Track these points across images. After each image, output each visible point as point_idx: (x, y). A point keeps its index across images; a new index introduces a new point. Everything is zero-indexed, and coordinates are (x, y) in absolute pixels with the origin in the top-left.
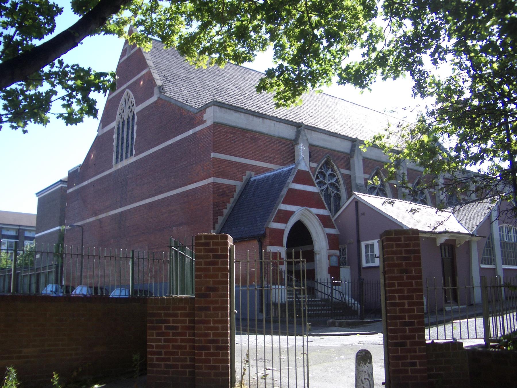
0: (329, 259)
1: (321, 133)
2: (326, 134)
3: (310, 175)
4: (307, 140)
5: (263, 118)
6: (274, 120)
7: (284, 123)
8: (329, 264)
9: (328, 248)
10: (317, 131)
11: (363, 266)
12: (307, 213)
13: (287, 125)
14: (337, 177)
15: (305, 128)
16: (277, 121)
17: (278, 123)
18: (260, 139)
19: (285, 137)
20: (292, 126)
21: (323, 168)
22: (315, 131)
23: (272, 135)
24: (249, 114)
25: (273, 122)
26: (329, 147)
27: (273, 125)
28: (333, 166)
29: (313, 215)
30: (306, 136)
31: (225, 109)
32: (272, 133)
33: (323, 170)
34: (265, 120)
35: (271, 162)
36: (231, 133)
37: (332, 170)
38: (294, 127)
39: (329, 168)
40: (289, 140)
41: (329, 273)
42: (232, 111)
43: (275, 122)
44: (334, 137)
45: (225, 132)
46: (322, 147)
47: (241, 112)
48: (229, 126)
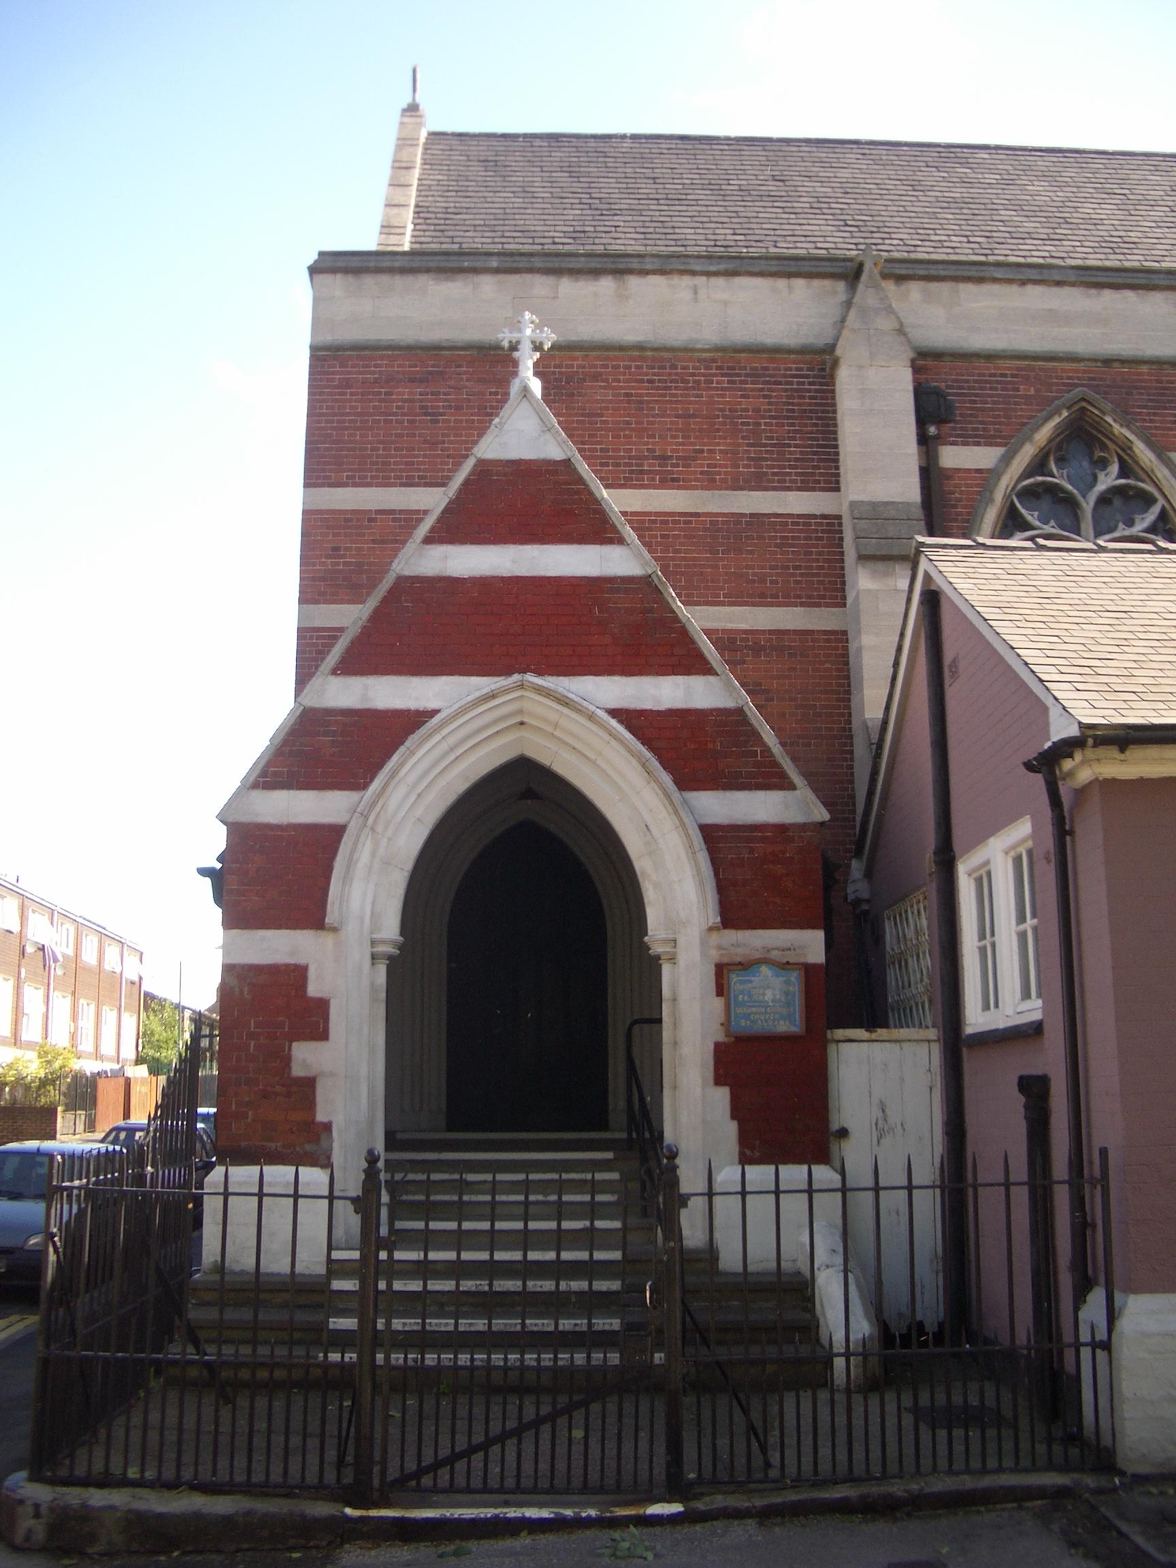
0: (721, 989)
1: (1023, 283)
2: (1059, 284)
3: (581, 480)
4: (901, 331)
5: (620, 272)
6: (693, 273)
7: (761, 274)
8: (726, 1024)
9: (715, 919)
10: (995, 280)
11: (969, 1030)
12: (544, 709)
13: (781, 283)
14: (1161, 502)
15: (885, 276)
16: (708, 274)
17: (720, 282)
18: (596, 377)
19: (769, 340)
20: (816, 283)
21: (1053, 466)
22: (980, 280)
23: (676, 344)
24: (531, 271)
25: (687, 281)
26: (1080, 348)
27: (687, 295)
28: (1127, 447)
29: (591, 717)
30: (890, 310)
31: (385, 279)
32: (677, 335)
33: (1059, 478)
34: (633, 281)
35: (669, 482)
36: (412, 381)
37: (1122, 462)
38: (827, 283)
39: (1103, 464)
40: (790, 351)
41: (719, 1081)
42: (423, 279)
43: (701, 281)
44: (1128, 293)
45: (376, 381)
46: (1036, 357)
47: (475, 271)
48: (400, 348)
